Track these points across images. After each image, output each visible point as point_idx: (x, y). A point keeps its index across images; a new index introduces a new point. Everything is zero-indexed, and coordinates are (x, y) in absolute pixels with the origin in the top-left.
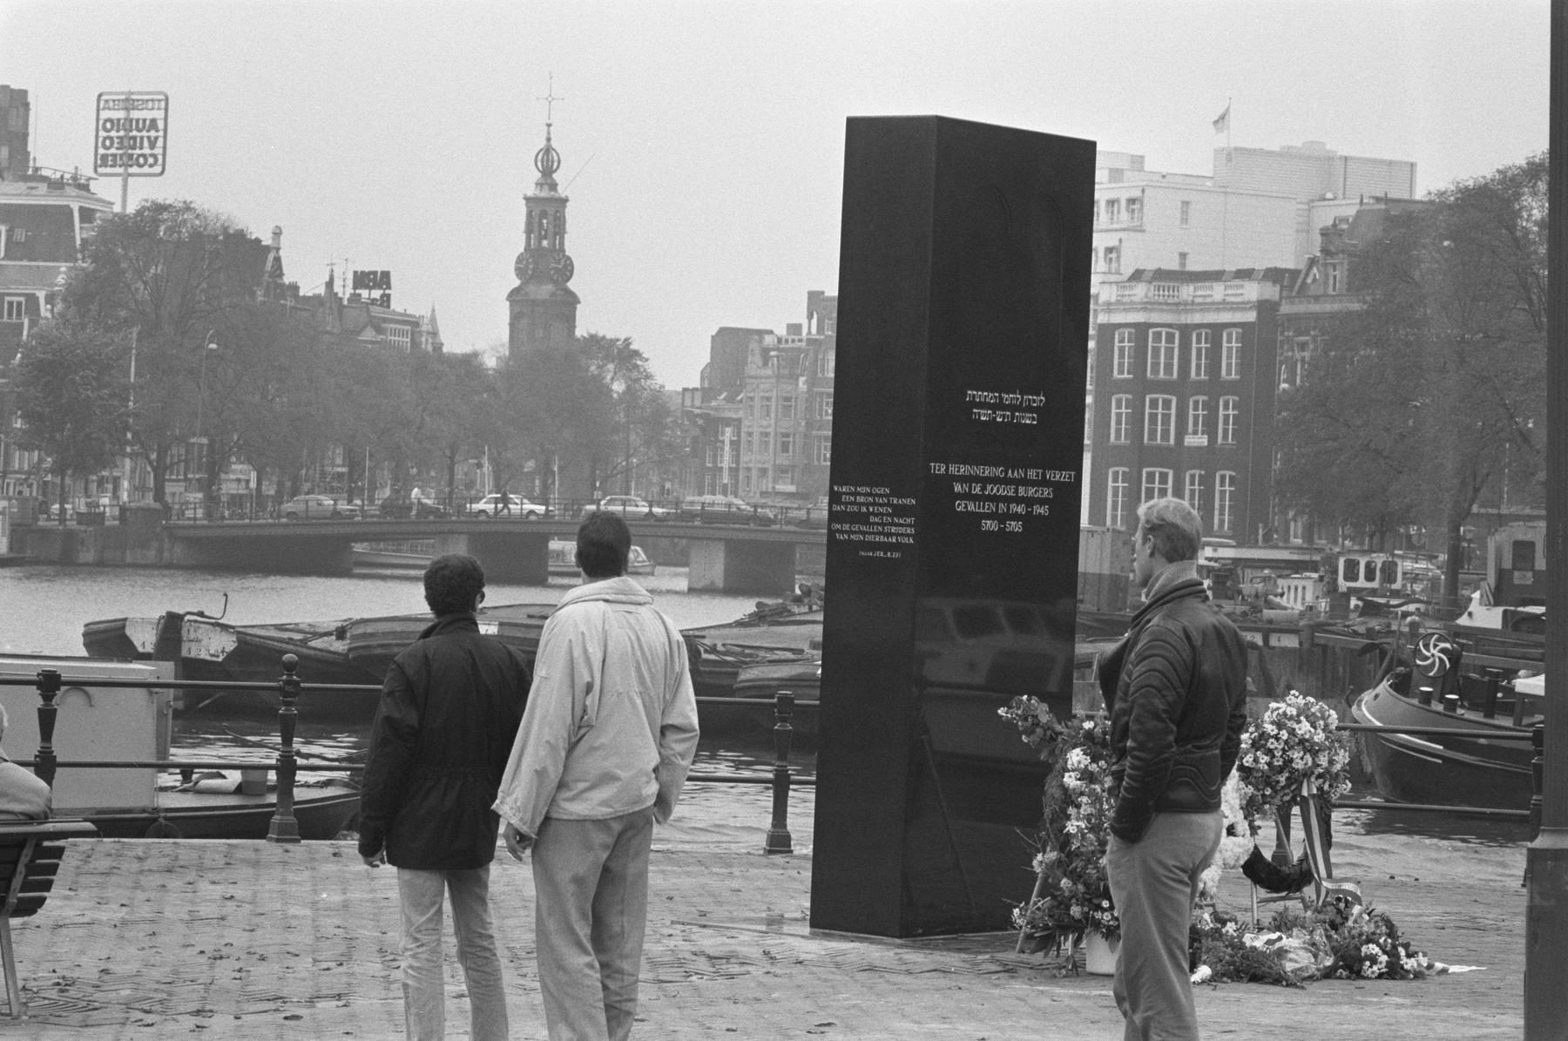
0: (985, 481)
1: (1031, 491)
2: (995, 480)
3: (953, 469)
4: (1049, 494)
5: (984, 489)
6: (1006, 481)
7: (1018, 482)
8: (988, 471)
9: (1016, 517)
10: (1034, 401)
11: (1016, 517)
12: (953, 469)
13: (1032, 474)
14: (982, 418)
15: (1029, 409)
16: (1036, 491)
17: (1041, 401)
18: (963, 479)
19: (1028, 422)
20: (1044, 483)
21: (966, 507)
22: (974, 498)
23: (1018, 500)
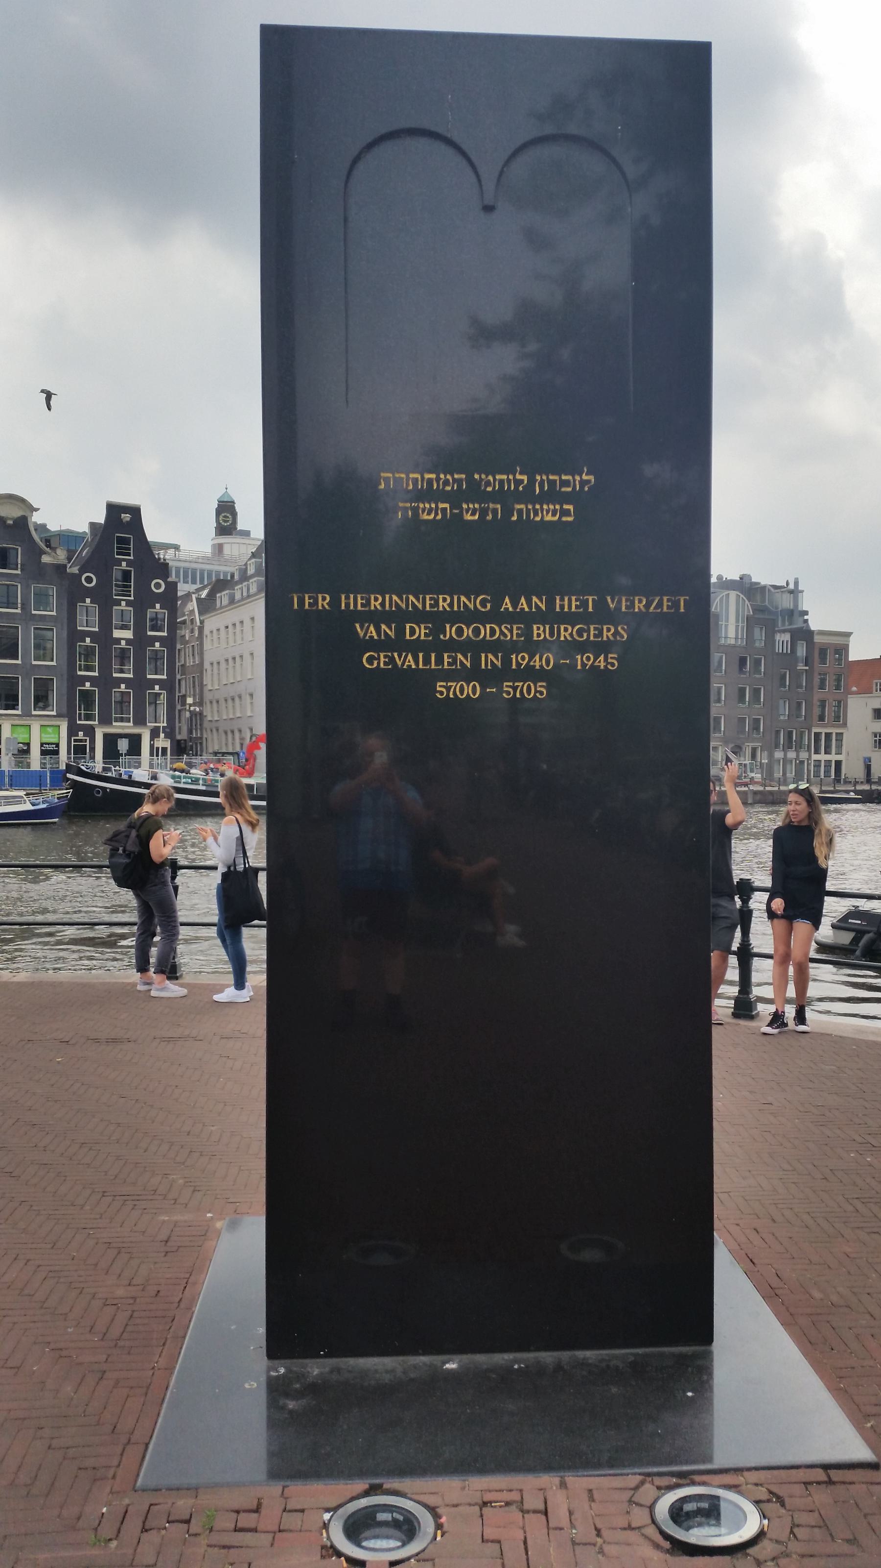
0: (438, 620)
1: (566, 632)
4: (616, 633)
6: (496, 617)
9: (530, 674)
10: (566, 483)
11: (530, 674)
12: (354, 602)
13: (570, 604)
15: (551, 495)
16: (580, 633)
17: (583, 483)
18: (376, 618)
19: (549, 518)
21: (392, 660)
22: (415, 647)
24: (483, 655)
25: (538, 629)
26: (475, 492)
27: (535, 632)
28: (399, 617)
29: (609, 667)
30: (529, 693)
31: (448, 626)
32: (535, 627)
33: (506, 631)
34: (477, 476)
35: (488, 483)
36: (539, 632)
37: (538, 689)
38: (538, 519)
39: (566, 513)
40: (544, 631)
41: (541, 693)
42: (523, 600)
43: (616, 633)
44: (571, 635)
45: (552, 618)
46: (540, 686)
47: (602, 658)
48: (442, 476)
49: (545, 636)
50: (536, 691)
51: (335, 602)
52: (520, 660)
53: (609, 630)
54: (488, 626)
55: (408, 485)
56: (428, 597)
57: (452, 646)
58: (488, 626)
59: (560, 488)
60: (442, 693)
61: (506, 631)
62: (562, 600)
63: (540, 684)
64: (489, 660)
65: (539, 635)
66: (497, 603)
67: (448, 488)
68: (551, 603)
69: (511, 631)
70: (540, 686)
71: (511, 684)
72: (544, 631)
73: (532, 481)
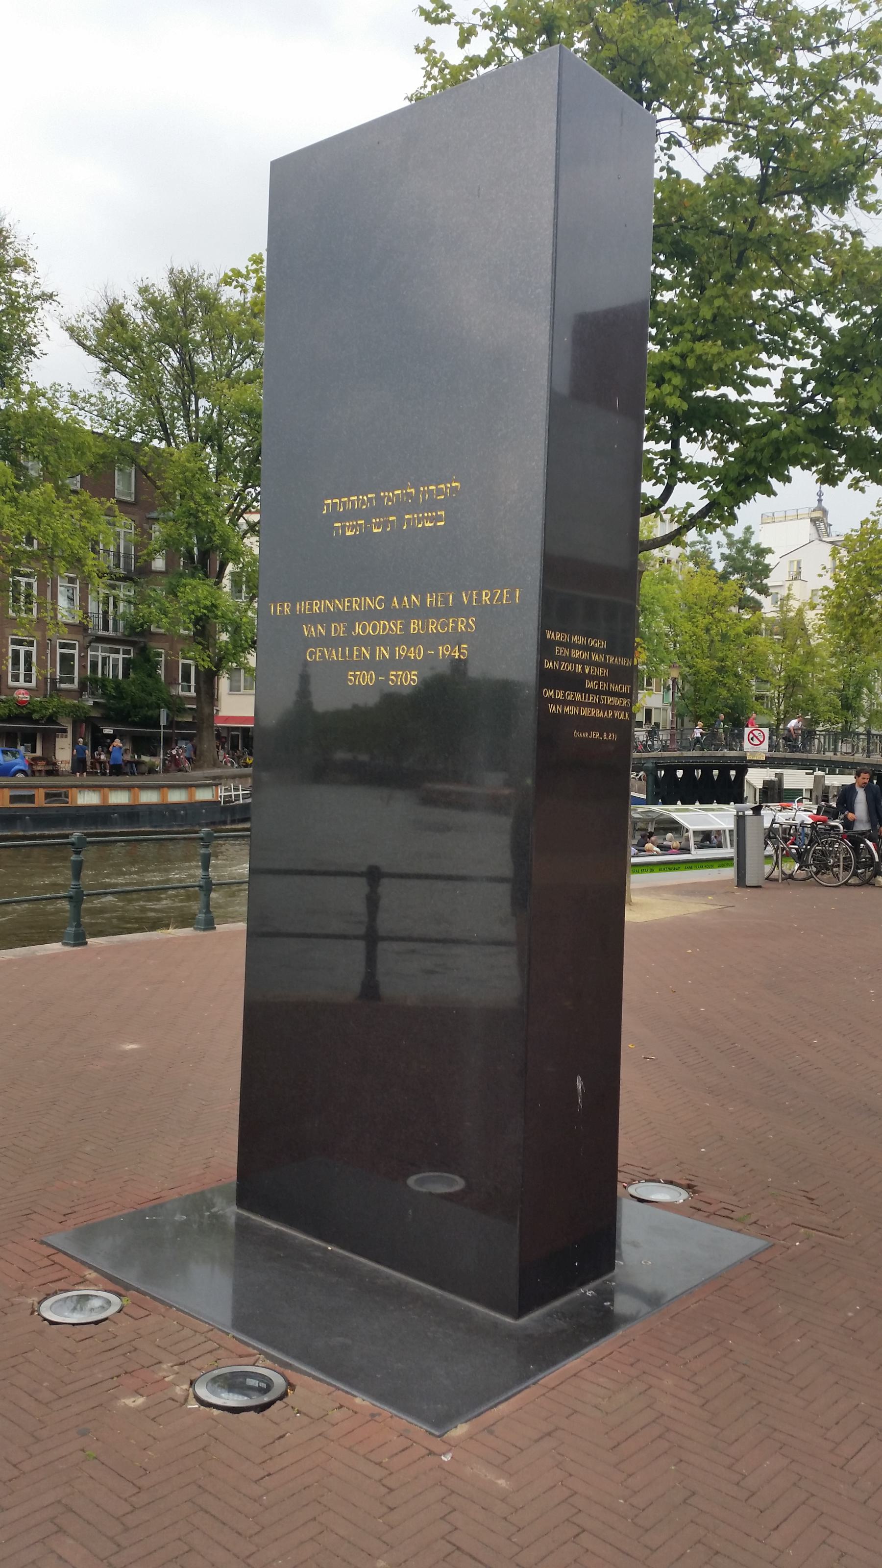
0: (350, 618)
2: (370, 615)
3: (302, 607)
4: (468, 625)
5: (350, 628)
6: (389, 614)
7: (406, 615)
8: (356, 604)
9: (406, 664)
10: (439, 492)
11: (406, 664)
14: (348, 533)
15: (432, 505)
18: (314, 619)
19: (428, 524)
20: (459, 610)
23: (408, 639)
24: (378, 648)
25: (414, 623)
26: (378, 510)
27: (412, 626)
28: (326, 618)
29: (462, 657)
30: (406, 681)
31: (357, 624)
32: (412, 621)
33: (392, 626)
34: (382, 494)
35: (389, 499)
36: (415, 626)
37: (413, 677)
38: (420, 526)
39: (439, 518)
40: (418, 625)
41: (414, 680)
42: (405, 598)
43: (468, 625)
44: (436, 628)
45: (424, 613)
46: (414, 675)
47: (457, 648)
48: (361, 497)
49: (419, 629)
50: (411, 679)
51: (293, 609)
52: (400, 651)
53: (462, 622)
54: (382, 622)
55: (340, 508)
56: (346, 600)
57: (362, 641)
58: (382, 622)
59: (437, 496)
60: (351, 680)
61: (392, 626)
62: (431, 597)
63: (413, 673)
64: (383, 652)
65: (414, 628)
66: (389, 601)
67: (364, 507)
68: (423, 601)
69: (395, 625)
70: (414, 675)
71: (395, 673)
72: (418, 625)
73: (418, 491)
